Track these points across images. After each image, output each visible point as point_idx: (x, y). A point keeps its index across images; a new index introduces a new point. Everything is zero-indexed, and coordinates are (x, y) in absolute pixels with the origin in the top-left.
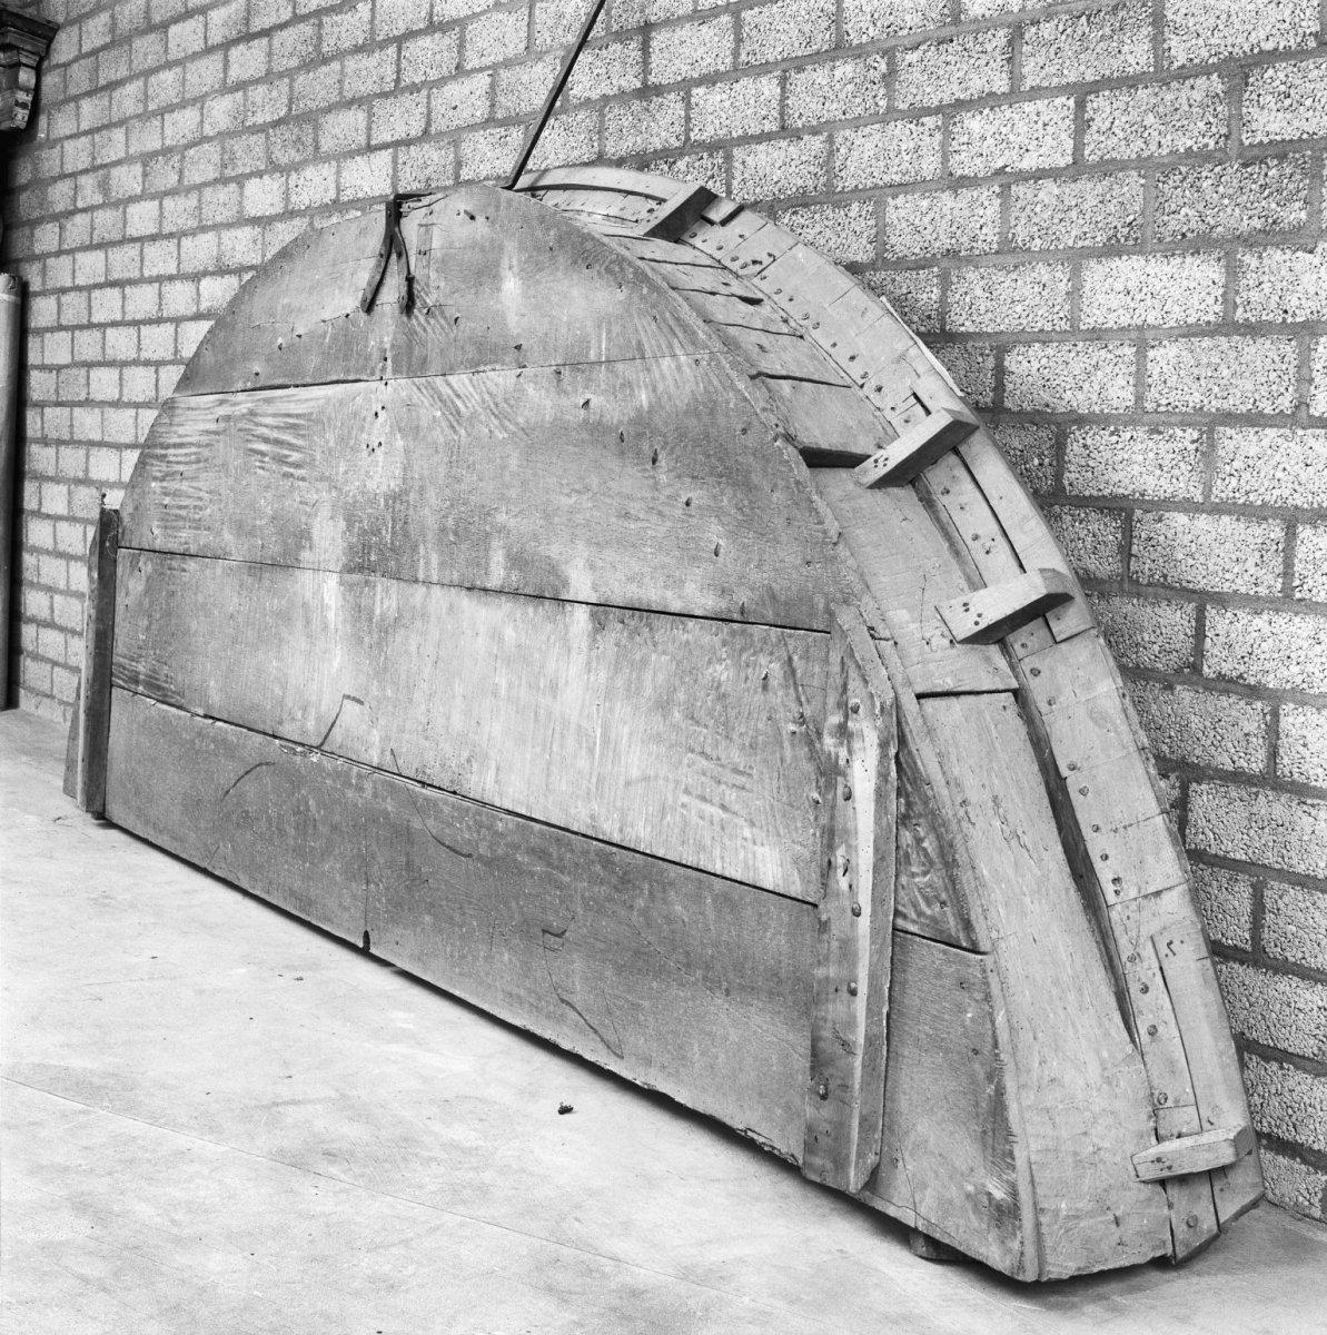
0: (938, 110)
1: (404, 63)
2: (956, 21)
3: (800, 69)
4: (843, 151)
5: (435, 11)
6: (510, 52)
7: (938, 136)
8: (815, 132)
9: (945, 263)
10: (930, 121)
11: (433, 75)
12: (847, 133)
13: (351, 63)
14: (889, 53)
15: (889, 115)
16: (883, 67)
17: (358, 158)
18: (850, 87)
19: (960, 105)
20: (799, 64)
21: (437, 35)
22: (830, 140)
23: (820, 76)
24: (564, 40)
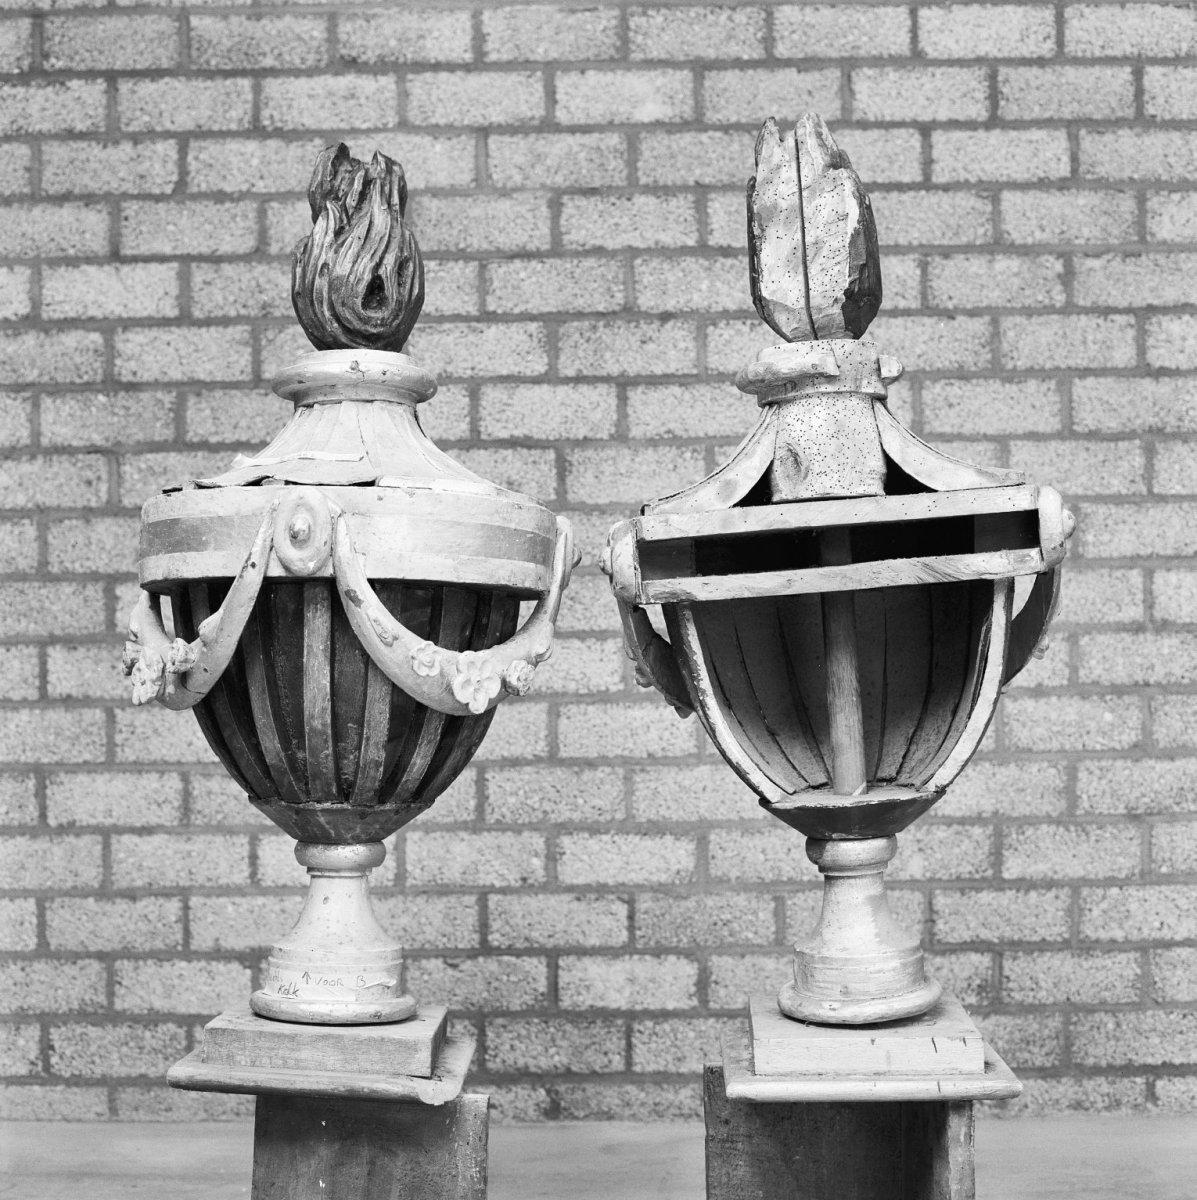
0: (1128, 311)
1: (193, 165)
2: (1143, 240)
3: (946, 256)
4: (1011, 334)
5: (265, 113)
6: (442, 180)
7: (1131, 333)
8: (973, 313)
9: (1148, 437)
10: (1120, 319)
11: (261, 187)
12: (1018, 319)
13: (55, 152)
14: (1066, 255)
15: (1069, 309)
16: (1059, 267)
17: (92, 270)
18: (1016, 281)
19: (1151, 309)
20: (947, 252)
21: (273, 143)
22: (995, 322)
23: (976, 265)
24: (548, 182)
